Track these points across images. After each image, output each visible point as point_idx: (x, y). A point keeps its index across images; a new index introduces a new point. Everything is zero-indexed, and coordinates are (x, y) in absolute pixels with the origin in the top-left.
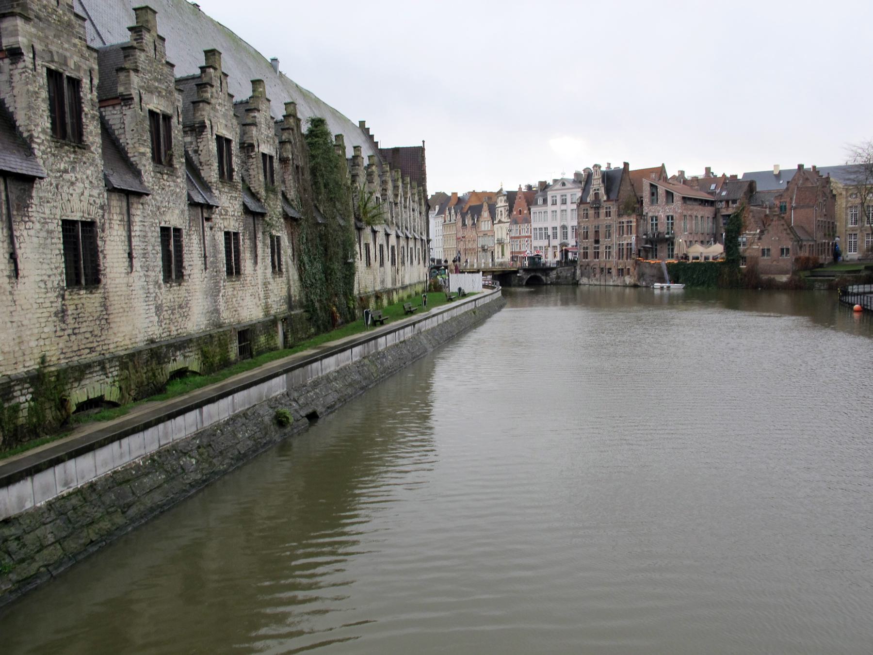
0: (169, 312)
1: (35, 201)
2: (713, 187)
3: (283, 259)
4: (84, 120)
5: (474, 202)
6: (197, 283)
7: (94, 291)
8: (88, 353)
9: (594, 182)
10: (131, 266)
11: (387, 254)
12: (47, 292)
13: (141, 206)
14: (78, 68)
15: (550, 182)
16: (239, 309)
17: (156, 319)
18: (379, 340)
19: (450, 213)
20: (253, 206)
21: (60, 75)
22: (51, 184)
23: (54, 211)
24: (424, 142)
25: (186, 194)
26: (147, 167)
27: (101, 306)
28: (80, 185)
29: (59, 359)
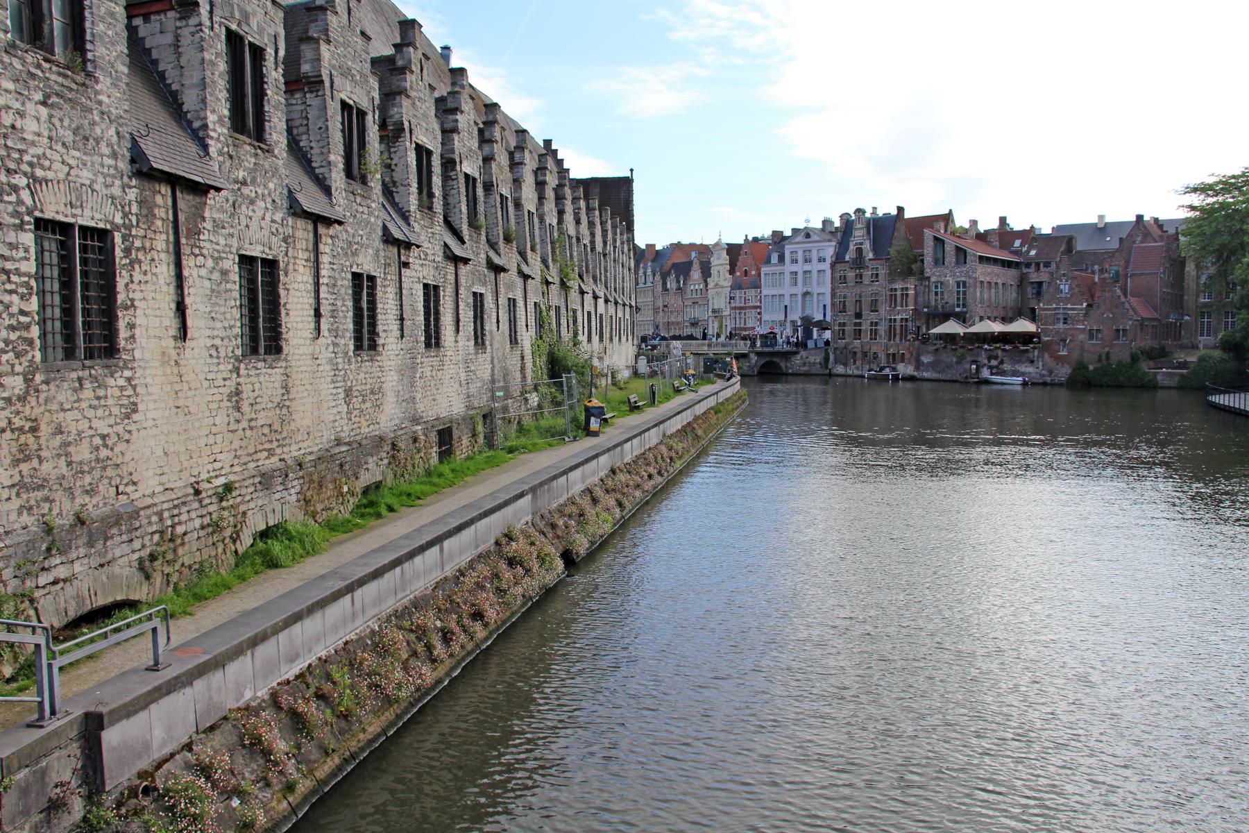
0: (360, 399)
1: (208, 225)
2: (1017, 243)
3: (487, 327)
4: (266, 108)
5: (679, 258)
6: (392, 358)
7: (274, 365)
8: (267, 458)
9: (857, 233)
10: (318, 329)
12: (219, 364)
13: (330, 241)
14: (261, 31)
15: (788, 233)
16: (438, 397)
17: (344, 408)
18: (625, 445)
20: (458, 251)
21: (241, 39)
22: (227, 200)
23: (229, 241)
24: (632, 170)
25: (381, 225)
27: (283, 388)
28: (261, 204)
29: (232, 466)
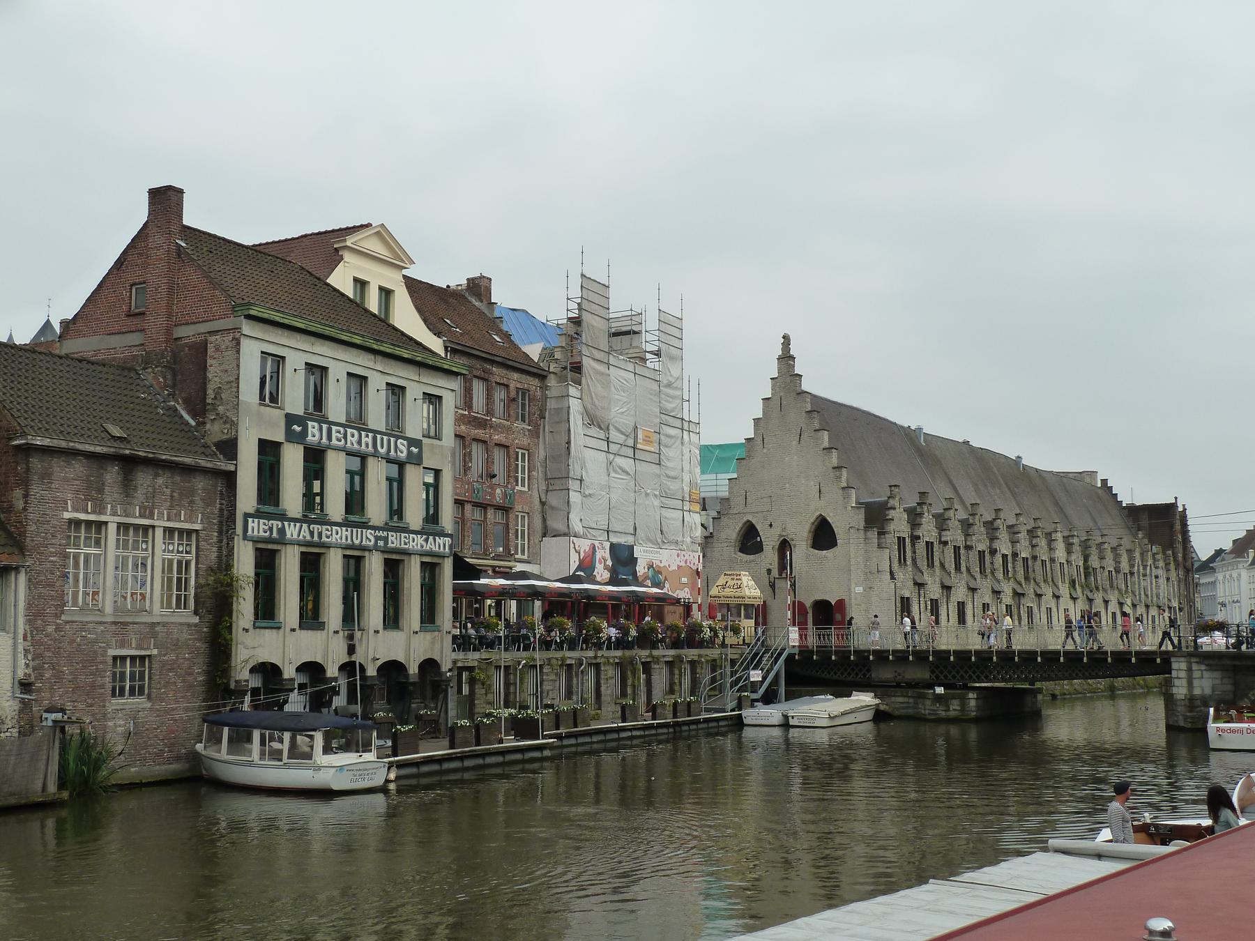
20: (1019, 591)
24: (1176, 498)
26: (978, 576)
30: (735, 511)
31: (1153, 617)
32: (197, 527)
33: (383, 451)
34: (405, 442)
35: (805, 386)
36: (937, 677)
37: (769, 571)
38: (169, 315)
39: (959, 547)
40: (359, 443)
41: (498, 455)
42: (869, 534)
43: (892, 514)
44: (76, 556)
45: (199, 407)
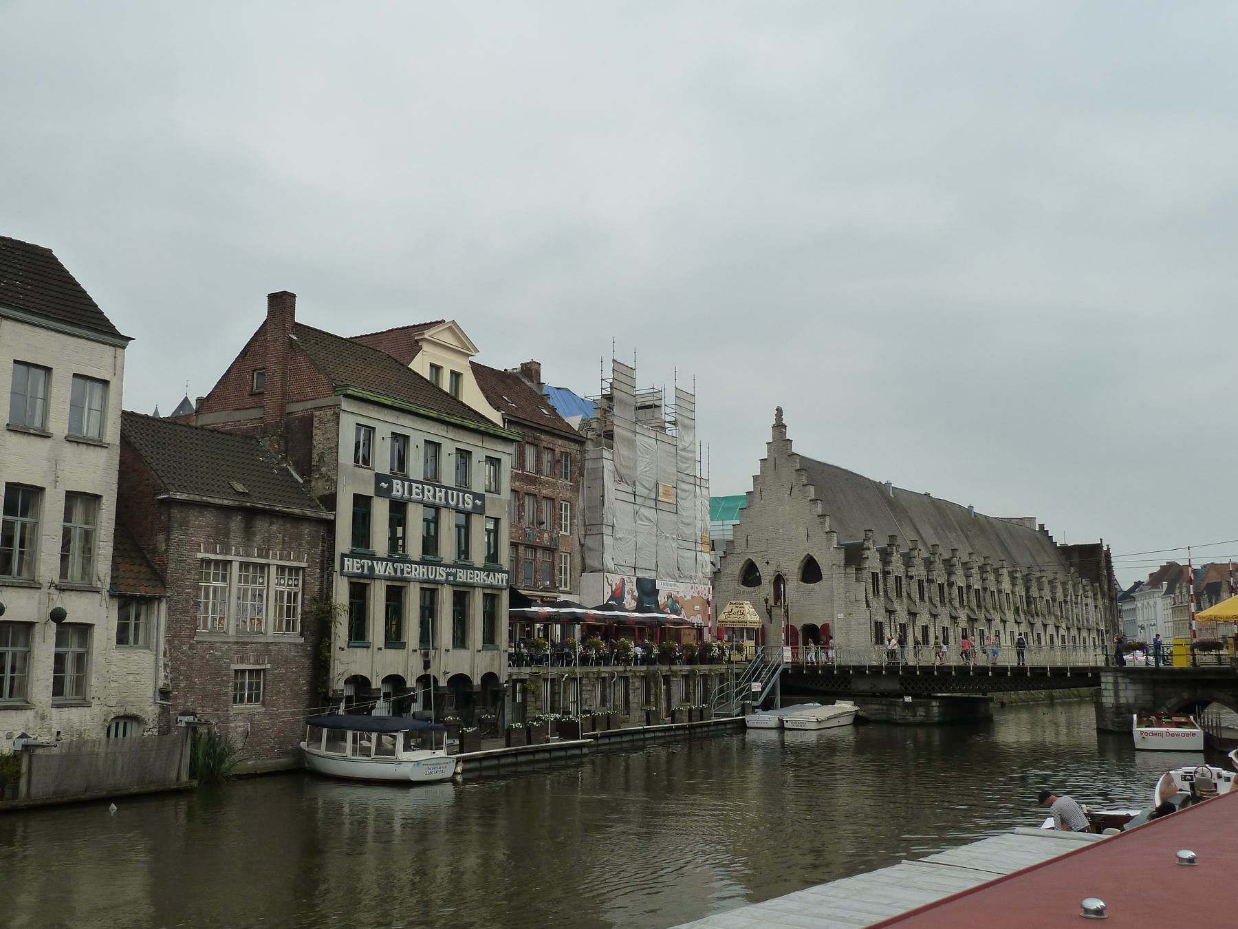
5: (1213, 578)
11: (1058, 642)
19: (1181, 593)
20: (973, 616)
24: (1101, 540)
26: (938, 604)
30: (738, 552)
31: (1084, 638)
32: (304, 565)
33: (453, 503)
34: (471, 496)
35: (795, 449)
36: (906, 688)
37: (767, 601)
38: (283, 394)
39: (923, 581)
40: (434, 497)
41: (546, 507)
42: (849, 570)
43: (867, 553)
44: (207, 589)
45: (306, 468)
